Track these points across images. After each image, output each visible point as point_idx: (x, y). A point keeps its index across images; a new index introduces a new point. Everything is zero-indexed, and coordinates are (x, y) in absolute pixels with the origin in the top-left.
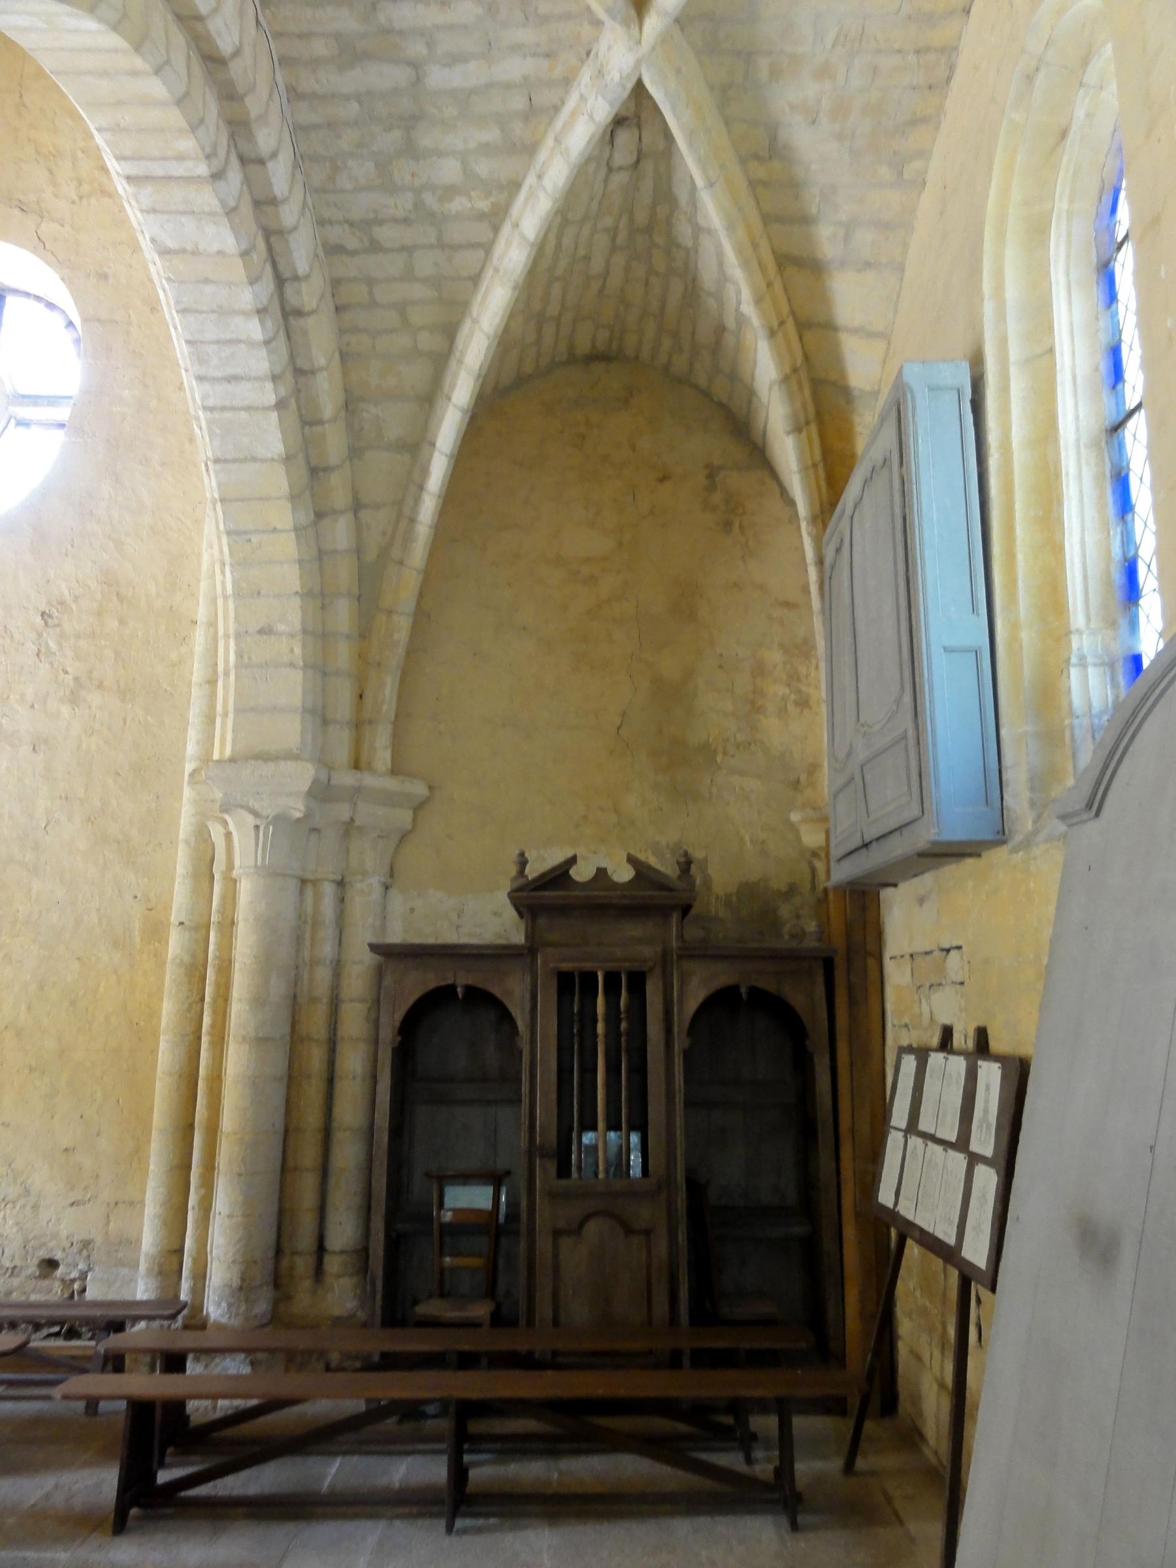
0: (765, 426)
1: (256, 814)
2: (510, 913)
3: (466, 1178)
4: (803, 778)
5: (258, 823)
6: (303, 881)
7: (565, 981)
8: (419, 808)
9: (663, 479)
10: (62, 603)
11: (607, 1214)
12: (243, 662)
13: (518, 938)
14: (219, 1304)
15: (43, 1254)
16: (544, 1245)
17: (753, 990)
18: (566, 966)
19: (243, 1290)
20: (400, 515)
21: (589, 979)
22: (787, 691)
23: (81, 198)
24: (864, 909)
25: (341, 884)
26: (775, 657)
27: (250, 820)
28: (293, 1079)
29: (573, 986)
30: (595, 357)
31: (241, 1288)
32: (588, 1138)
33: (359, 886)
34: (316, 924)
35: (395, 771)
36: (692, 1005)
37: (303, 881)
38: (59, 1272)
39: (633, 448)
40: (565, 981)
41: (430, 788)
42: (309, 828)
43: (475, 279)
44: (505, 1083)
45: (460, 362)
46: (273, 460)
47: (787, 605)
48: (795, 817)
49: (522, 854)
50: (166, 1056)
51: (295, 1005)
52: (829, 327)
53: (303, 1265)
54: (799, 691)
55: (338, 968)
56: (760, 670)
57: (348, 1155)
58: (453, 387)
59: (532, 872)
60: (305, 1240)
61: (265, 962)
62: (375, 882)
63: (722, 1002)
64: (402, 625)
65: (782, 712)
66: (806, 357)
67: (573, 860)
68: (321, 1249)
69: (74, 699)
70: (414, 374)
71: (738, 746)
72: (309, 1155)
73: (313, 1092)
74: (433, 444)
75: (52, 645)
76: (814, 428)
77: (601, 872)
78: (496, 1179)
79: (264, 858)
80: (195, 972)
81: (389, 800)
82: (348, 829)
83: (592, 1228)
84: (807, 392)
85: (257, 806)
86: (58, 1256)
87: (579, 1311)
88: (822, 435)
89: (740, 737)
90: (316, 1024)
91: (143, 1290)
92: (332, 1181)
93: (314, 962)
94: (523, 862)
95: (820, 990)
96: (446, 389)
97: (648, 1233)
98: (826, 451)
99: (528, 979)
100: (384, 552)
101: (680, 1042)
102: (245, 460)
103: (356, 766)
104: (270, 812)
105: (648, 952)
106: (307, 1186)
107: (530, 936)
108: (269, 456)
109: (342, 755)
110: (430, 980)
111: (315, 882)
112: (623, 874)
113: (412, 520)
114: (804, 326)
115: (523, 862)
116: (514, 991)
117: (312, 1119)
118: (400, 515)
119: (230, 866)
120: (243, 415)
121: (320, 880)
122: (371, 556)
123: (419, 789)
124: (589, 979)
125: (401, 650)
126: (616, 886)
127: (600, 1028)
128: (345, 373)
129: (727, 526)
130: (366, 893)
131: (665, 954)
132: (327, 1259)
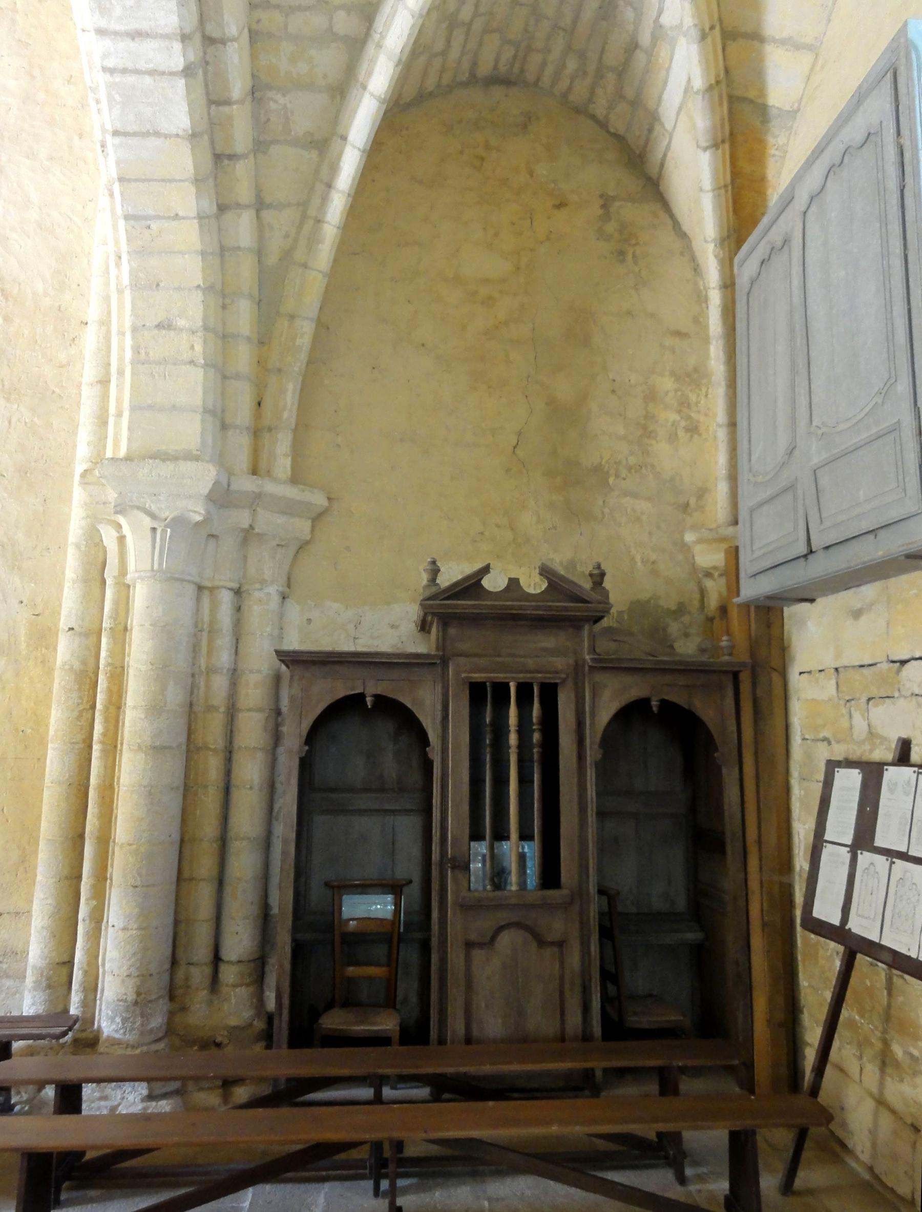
0: (665, 155)
1: (153, 516)
3: (365, 888)
4: (693, 502)
5: (155, 526)
6: (200, 588)
7: (477, 691)
8: (318, 518)
9: (560, 206)
11: (518, 925)
12: (140, 359)
13: (420, 646)
14: (112, 1020)
16: (456, 958)
17: (664, 703)
18: (478, 677)
19: (139, 1004)
20: (304, 217)
21: (501, 690)
22: (678, 418)
24: (769, 626)
25: (238, 592)
26: (666, 384)
27: (147, 522)
28: (189, 789)
29: (485, 696)
30: (499, 80)
31: (136, 1003)
33: (257, 594)
34: (213, 631)
35: (295, 479)
36: (605, 715)
37: (200, 588)
39: (531, 173)
40: (477, 691)
41: (329, 499)
42: (205, 534)
45: (379, 46)
46: (177, 135)
47: (678, 334)
48: (689, 537)
49: (434, 562)
50: (55, 764)
51: (192, 714)
52: (756, 37)
53: (199, 975)
54: (690, 417)
55: (235, 675)
56: (651, 396)
57: (243, 864)
58: (369, 74)
59: (446, 579)
60: (201, 951)
61: (162, 670)
62: (273, 590)
63: (632, 714)
64: (306, 330)
65: (673, 438)
67: (486, 570)
68: (217, 959)
70: (327, 61)
71: (630, 469)
72: (205, 865)
73: (210, 801)
74: (344, 138)
76: (727, 146)
77: (514, 583)
78: (395, 888)
79: (160, 564)
80: (86, 679)
81: (289, 508)
82: (248, 536)
83: (506, 940)
85: (154, 508)
87: (493, 1025)
89: (632, 460)
90: (213, 732)
92: (228, 890)
93: (211, 671)
94: (435, 571)
95: (729, 701)
96: (361, 78)
97: (560, 944)
98: (736, 174)
99: (439, 688)
100: (287, 255)
101: (593, 754)
102: (146, 134)
103: (254, 472)
104: (169, 514)
105: (560, 663)
106: (204, 895)
108: (174, 131)
109: (242, 460)
110: (341, 691)
111: (212, 590)
112: (533, 584)
113: (319, 221)
116: (424, 700)
117: (209, 829)
118: (304, 217)
119: (123, 571)
120: (148, 80)
121: (218, 588)
122: (272, 259)
123: (319, 500)
124: (501, 690)
125: (303, 356)
126: (528, 597)
127: (513, 739)
128: (253, 56)
129: (621, 254)
130: (263, 604)
131: (578, 667)
132: (223, 968)
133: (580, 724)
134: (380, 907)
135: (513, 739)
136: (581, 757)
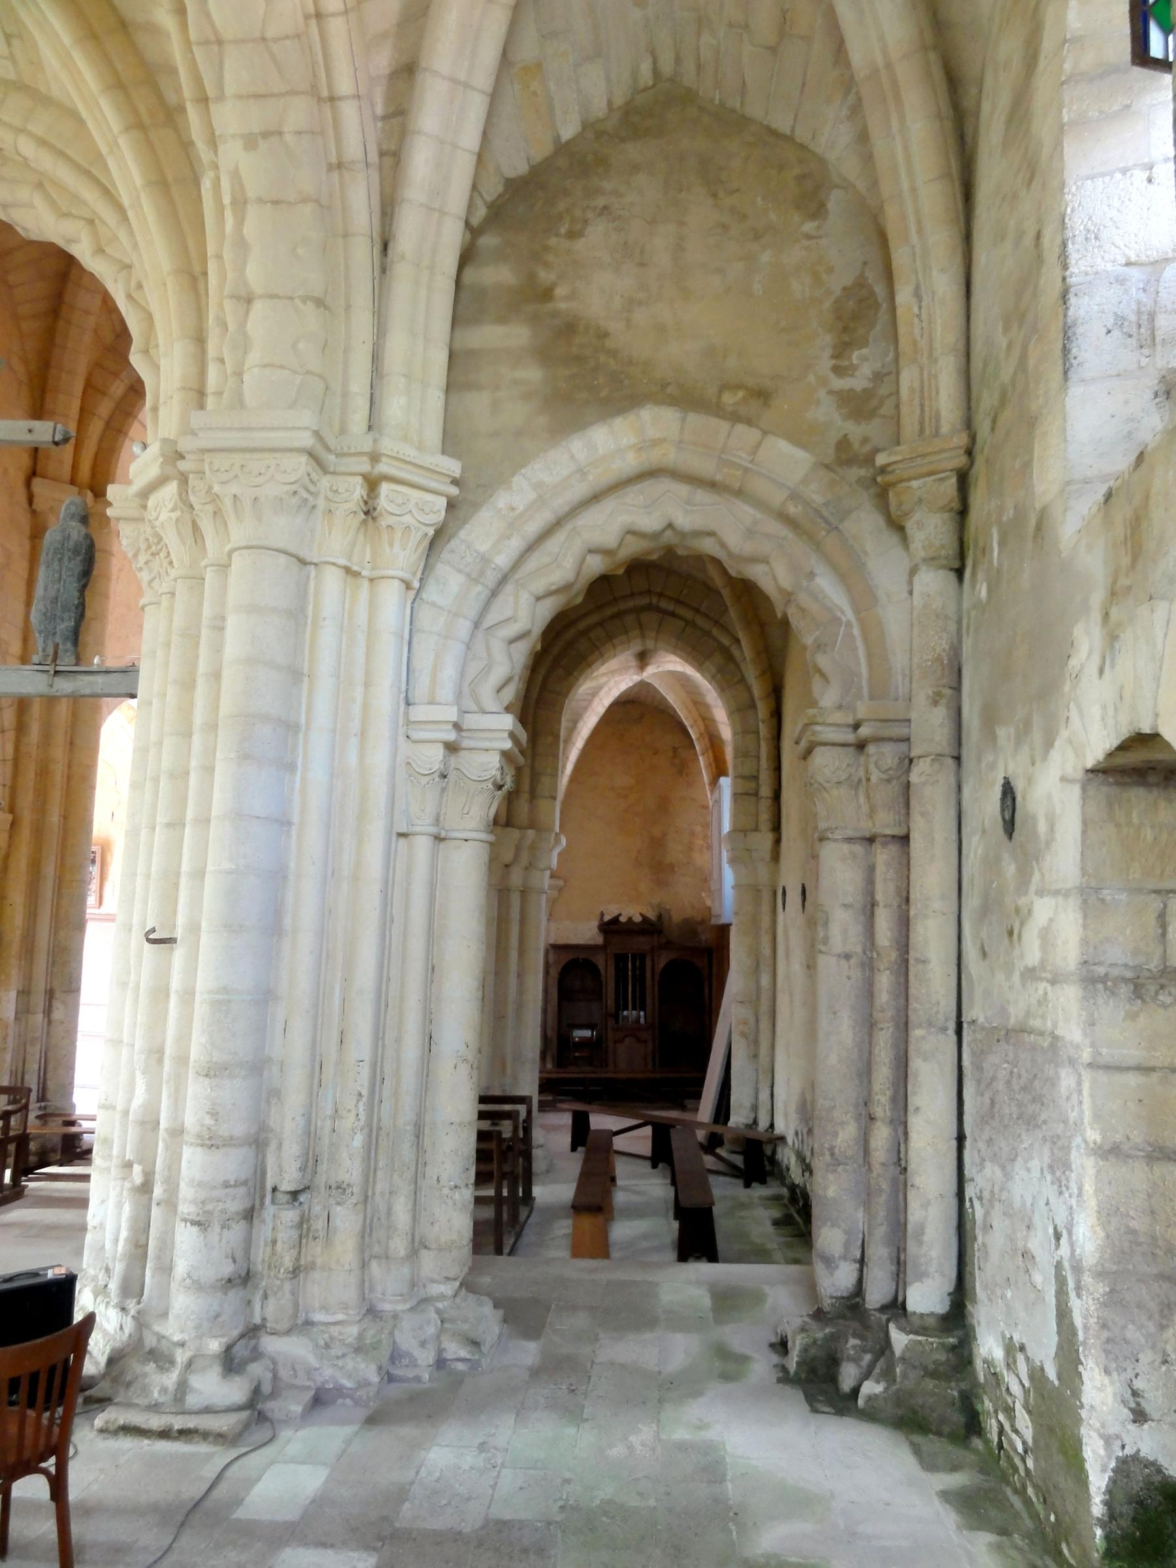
2: (595, 930)
8: (560, 890)
9: (656, 753)
13: (599, 940)
16: (611, 1045)
26: (698, 829)
29: (620, 959)
32: (625, 1013)
36: (661, 966)
43: (586, 708)
44: (597, 994)
48: (703, 895)
56: (692, 834)
59: (607, 918)
66: (706, 727)
76: (710, 751)
77: (630, 919)
78: (591, 1027)
83: (627, 1040)
84: (707, 739)
88: (714, 752)
94: (602, 915)
98: (715, 757)
101: (657, 978)
107: (605, 939)
112: (638, 919)
114: (704, 719)
115: (602, 915)
116: (600, 960)
123: (561, 883)
126: (635, 924)
134: (587, 1033)
136: (653, 979)
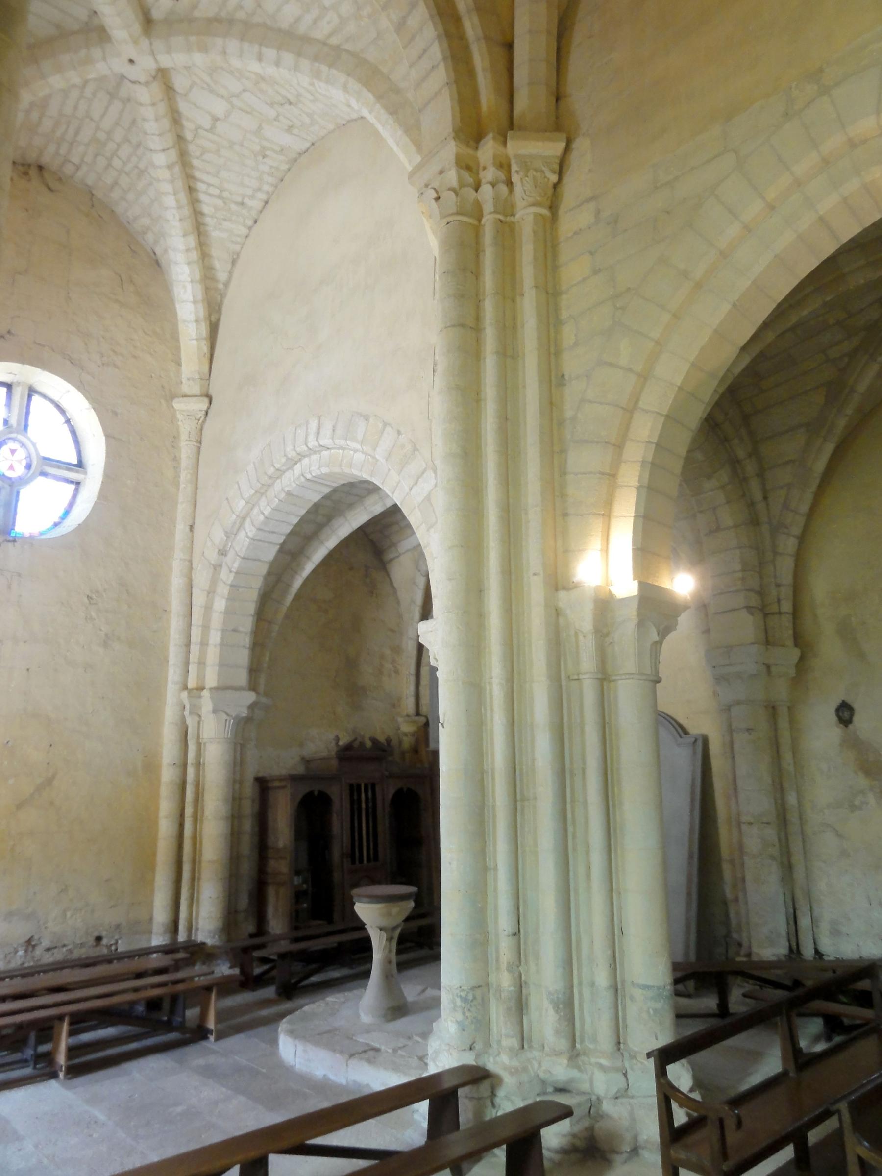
0: (394, 558)
1: (228, 715)
7: (351, 786)
9: (351, 569)
10: (98, 592)
12: (223, 645)
15: (96, 934)
23: (103, 364)
26: (388, 652)
27: (225, 717)
29: (354, 789)
36: (390, 796)
38: (104, 942)
40: (351, 786)
47: (392, 630)
50: (165, 828)
56: (382, 657)
63: (399, 793)
69: (105, 644)
75: (93, 614)
86: (104, 934)
91: (158, 940)
102: (255, 560)
120: (266, 545)
124: (359, 786)
127: (363, 805)
133: (383, 799)
135: (363, 805)
